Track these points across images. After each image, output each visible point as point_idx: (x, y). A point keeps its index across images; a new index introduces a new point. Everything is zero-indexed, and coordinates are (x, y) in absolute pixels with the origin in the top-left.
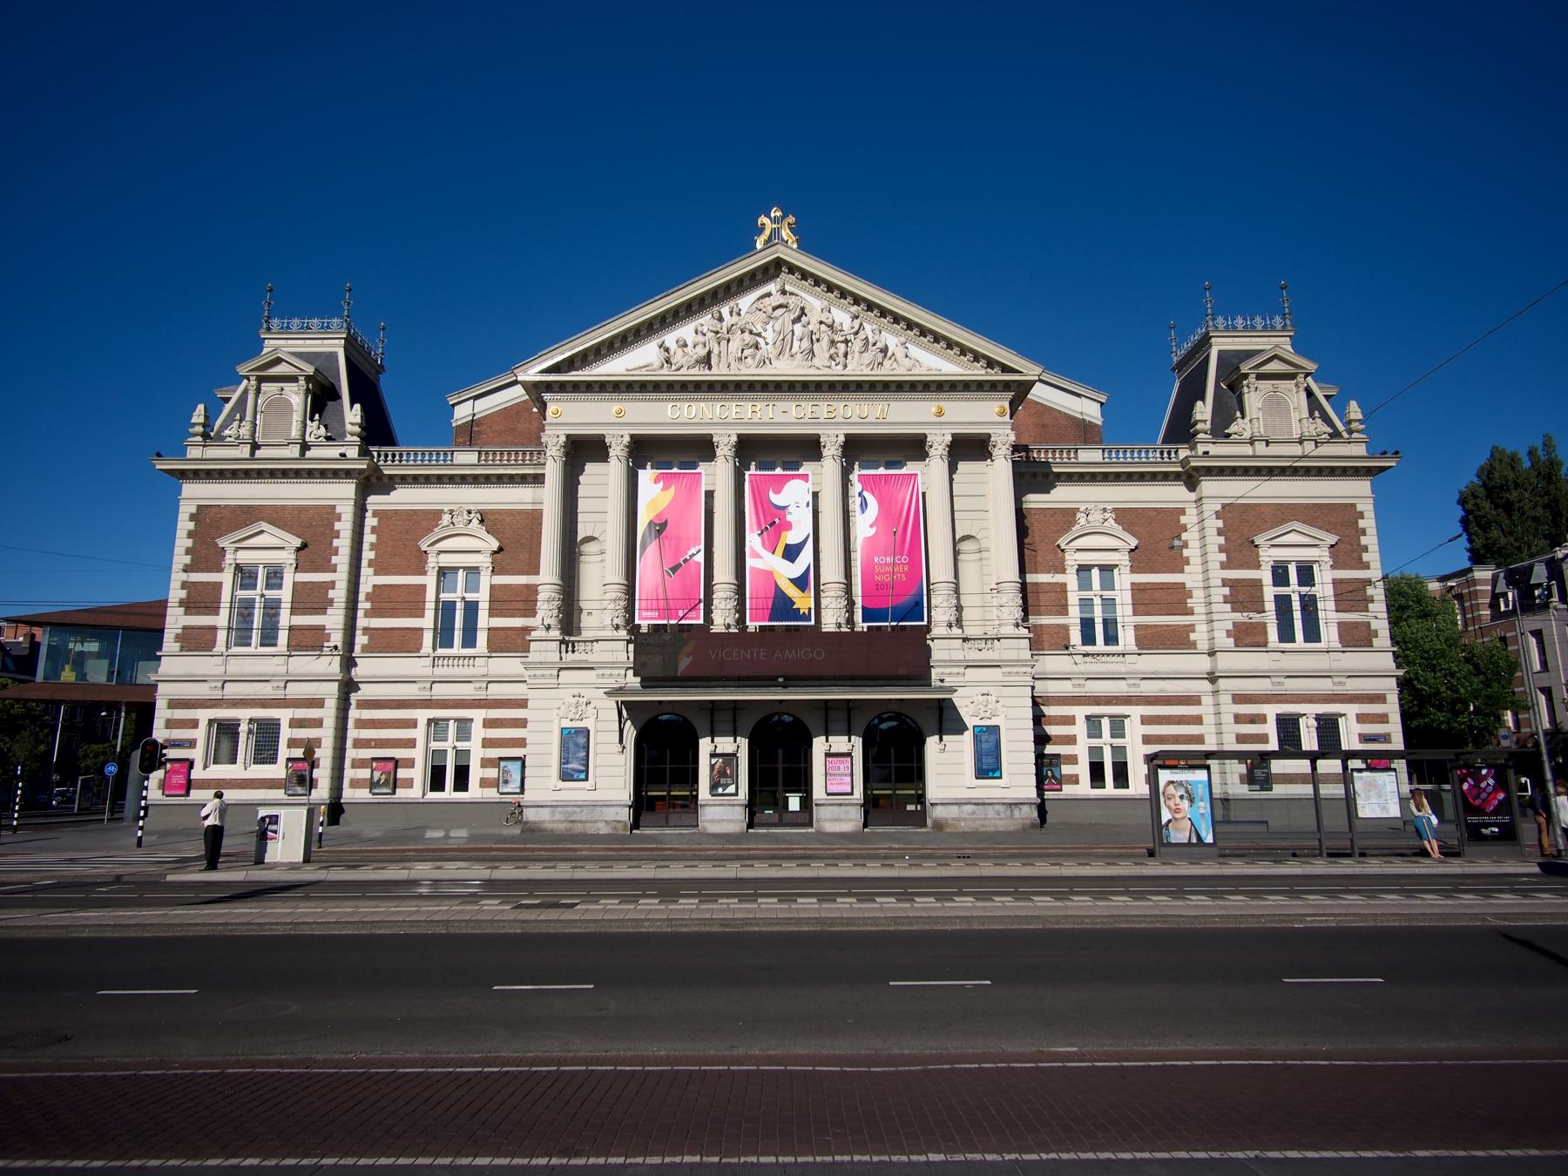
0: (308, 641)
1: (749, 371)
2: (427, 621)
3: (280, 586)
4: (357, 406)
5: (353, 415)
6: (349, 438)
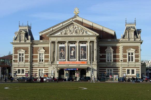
0: (26, 61)
1: (69, 34)
2: (38, 59)
3: (23, 55)
4: (30, 36)
5: (29, 37)
6: (29, 40)
